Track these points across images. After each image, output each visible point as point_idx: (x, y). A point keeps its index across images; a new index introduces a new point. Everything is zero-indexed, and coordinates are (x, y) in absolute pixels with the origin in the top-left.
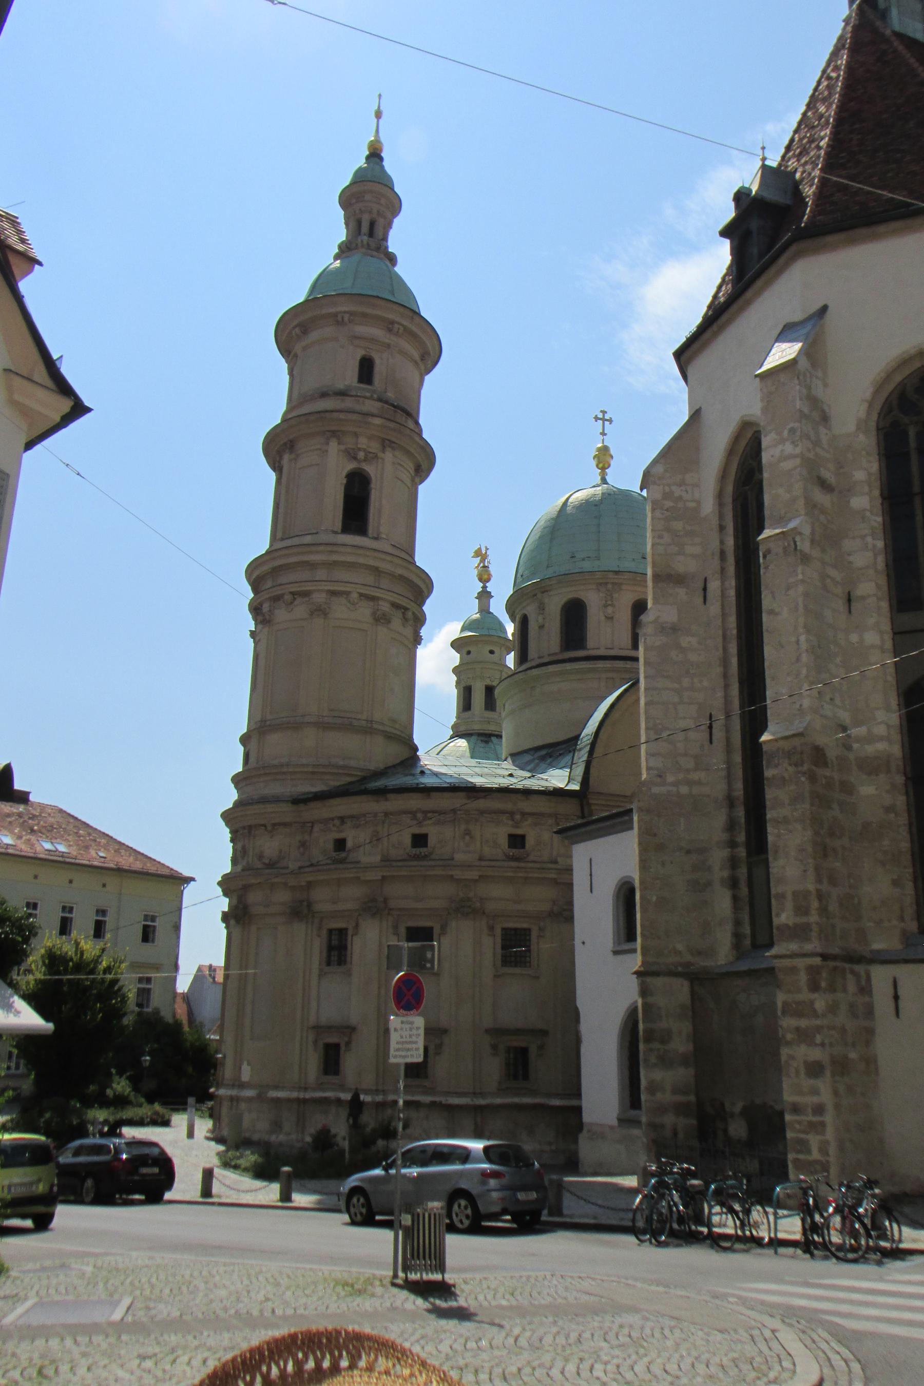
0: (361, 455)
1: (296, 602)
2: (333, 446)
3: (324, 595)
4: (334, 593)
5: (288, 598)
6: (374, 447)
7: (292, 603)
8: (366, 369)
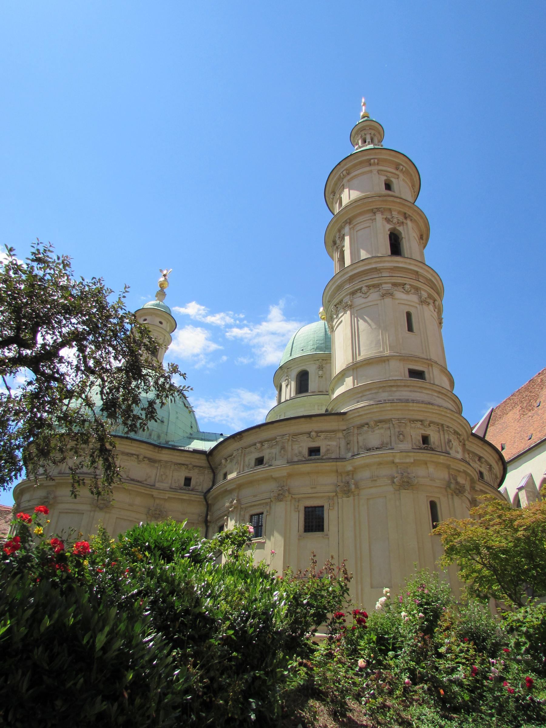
0: (395, 220)
1: (371, 291)
2: (379, 217)
3: (390, 285)
4: (395, 285)
5: (364, 289)
6: (401, 218)
7: (368, 292)
8: (388, 186)
